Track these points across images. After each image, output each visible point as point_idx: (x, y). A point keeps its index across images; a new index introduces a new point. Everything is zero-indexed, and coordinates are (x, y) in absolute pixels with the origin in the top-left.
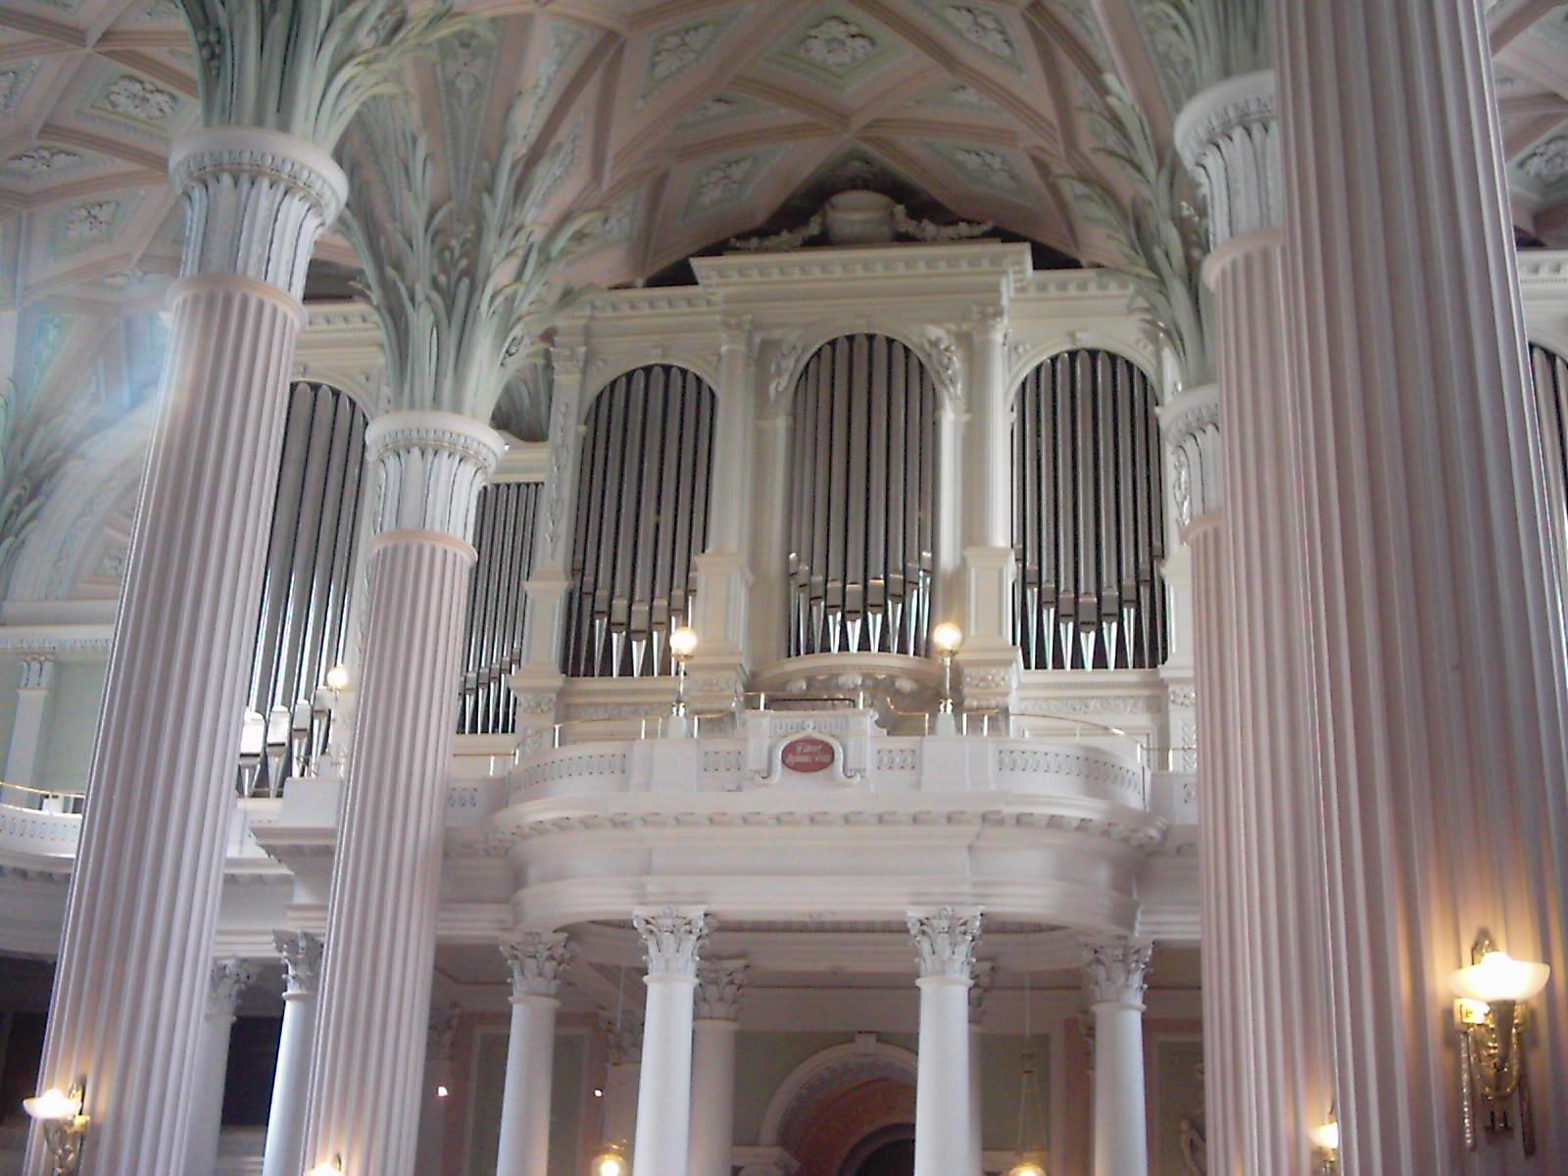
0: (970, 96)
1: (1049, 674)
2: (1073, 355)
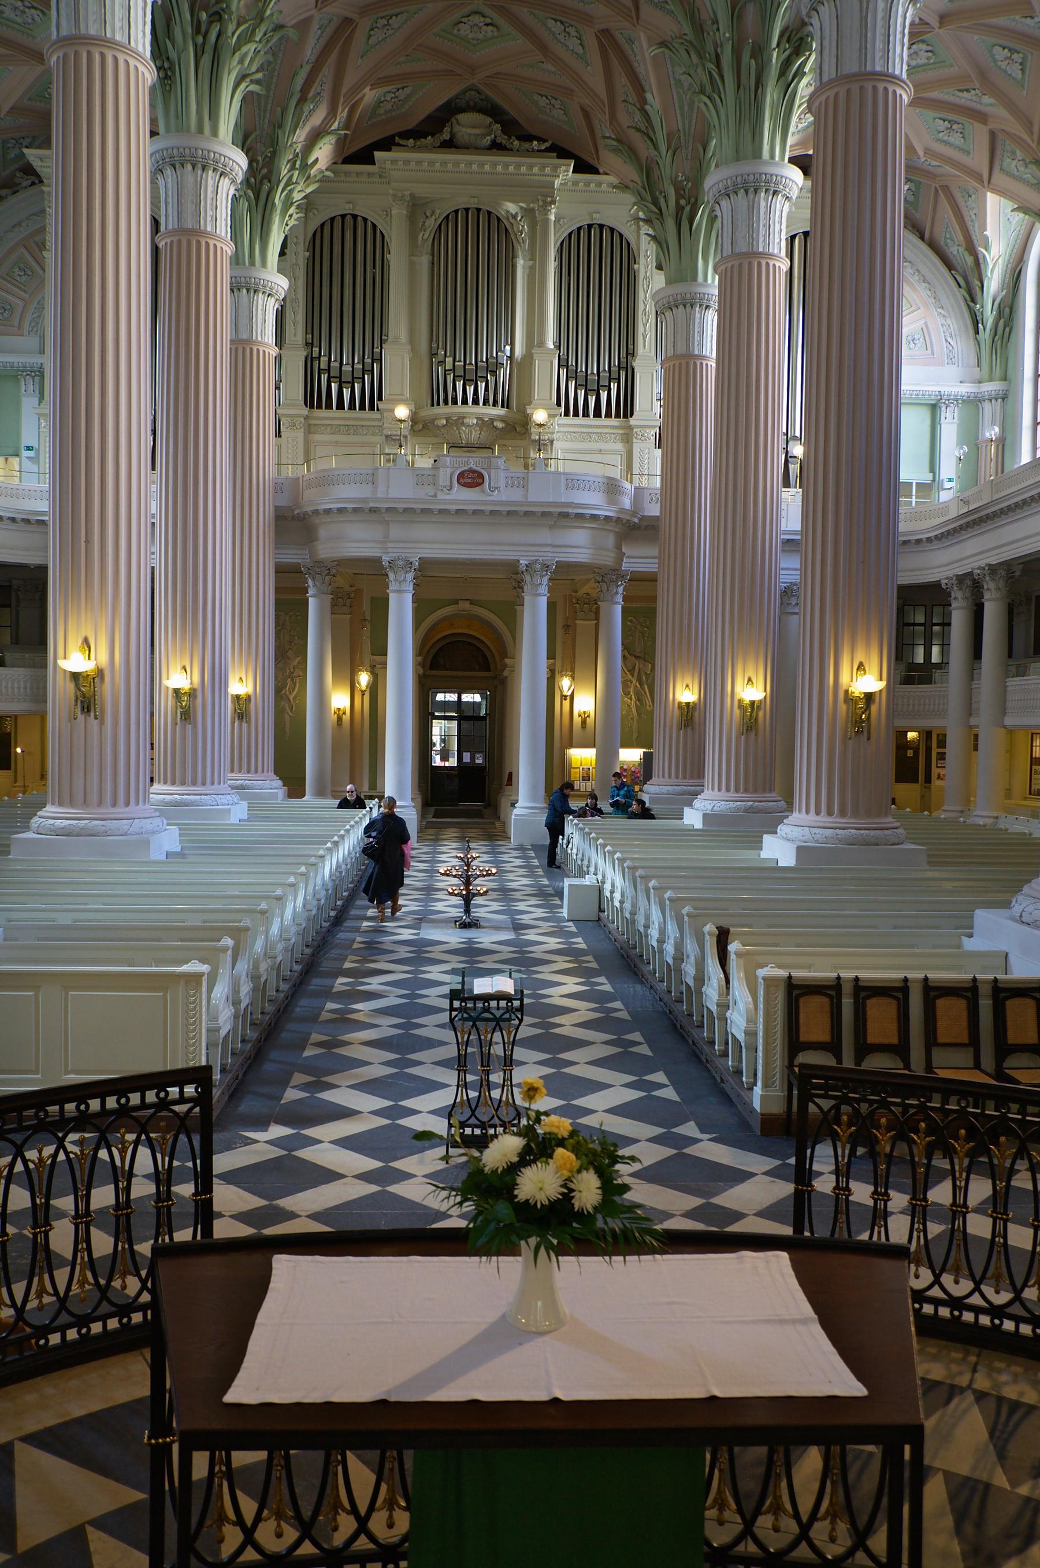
0: (550, 67)
1: (571, 420)
2: (590, 226)
